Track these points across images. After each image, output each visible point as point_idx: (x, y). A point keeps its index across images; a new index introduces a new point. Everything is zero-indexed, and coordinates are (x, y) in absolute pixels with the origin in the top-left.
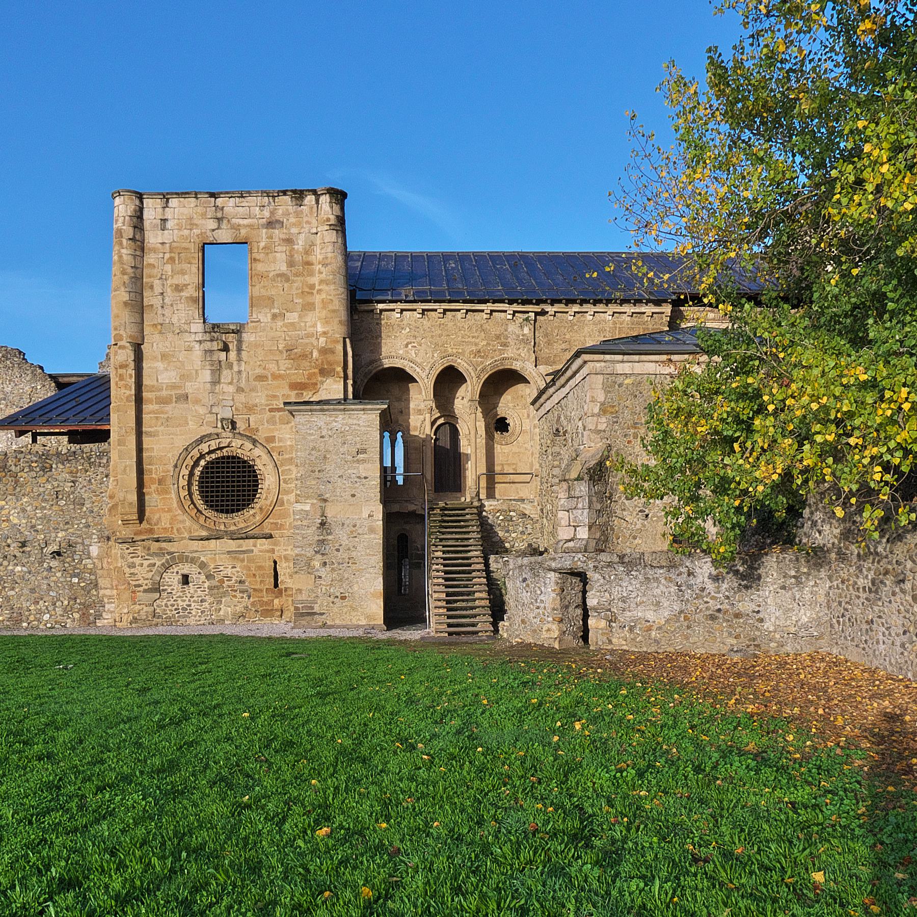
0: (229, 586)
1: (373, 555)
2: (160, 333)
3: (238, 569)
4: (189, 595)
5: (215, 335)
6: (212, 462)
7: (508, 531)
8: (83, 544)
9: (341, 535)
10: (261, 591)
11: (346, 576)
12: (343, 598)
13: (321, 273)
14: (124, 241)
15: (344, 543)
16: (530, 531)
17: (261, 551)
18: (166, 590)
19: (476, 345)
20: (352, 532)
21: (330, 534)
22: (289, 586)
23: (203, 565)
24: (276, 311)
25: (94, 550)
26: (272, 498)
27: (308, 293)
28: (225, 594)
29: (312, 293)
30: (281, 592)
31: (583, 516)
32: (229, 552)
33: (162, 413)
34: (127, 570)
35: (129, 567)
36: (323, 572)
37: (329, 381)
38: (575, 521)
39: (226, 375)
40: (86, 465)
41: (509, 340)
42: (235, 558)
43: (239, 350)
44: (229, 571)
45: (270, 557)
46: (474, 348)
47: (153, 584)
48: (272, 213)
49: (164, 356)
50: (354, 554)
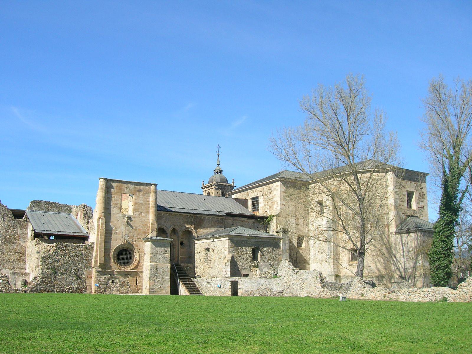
9: (160, 272)
19: (181, 223)
26: (137, 260)
30: (138, 285)
46: (180, 224)
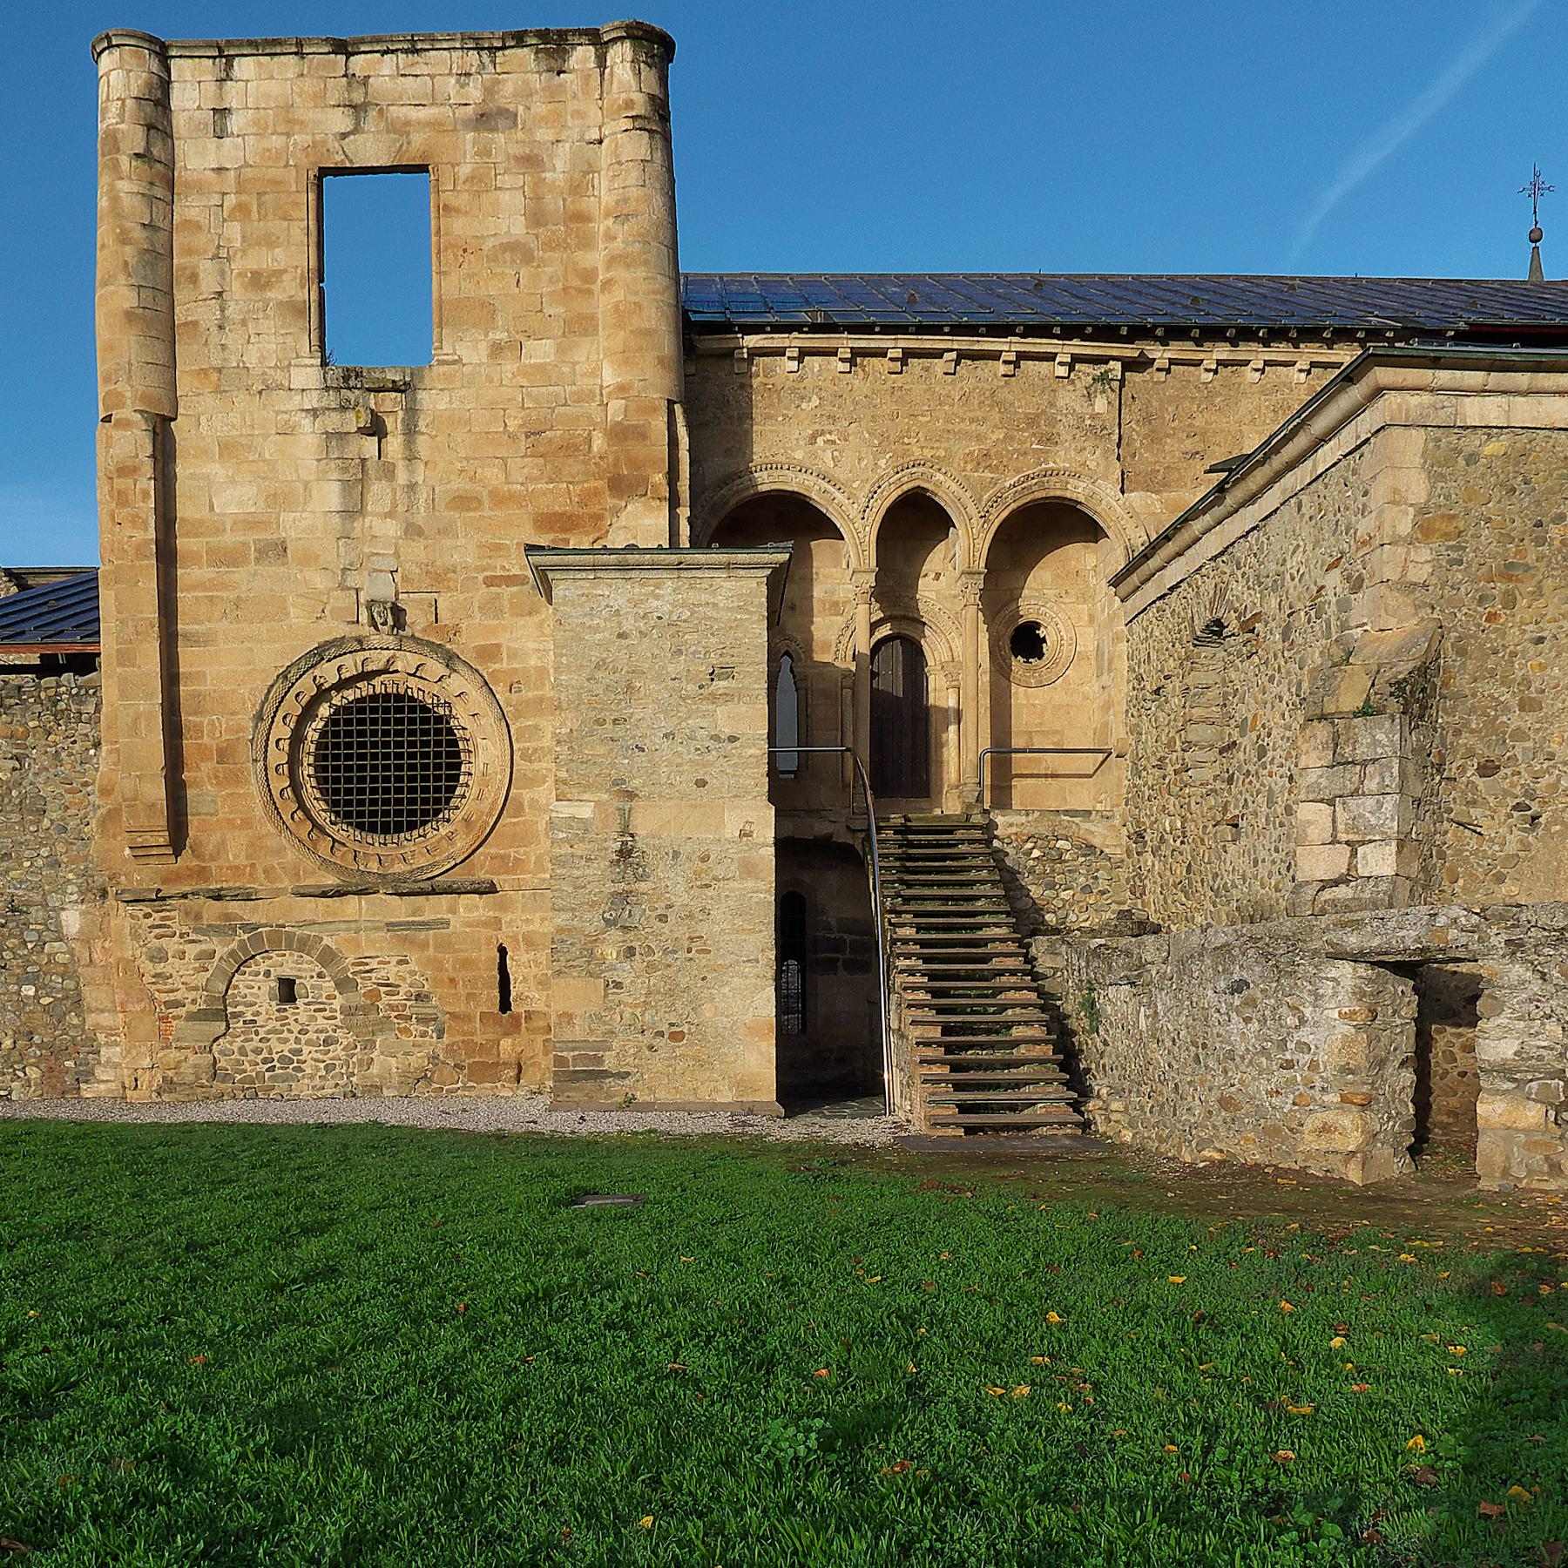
0: (392, 1007)
1: (753, 931)
2: (218, 390)
3: (412, 966)
4: (296, 1028)
5: (352, 396)
6: (347, 709)
8: (44, 905)
9: (670, 882)
10: (467, 1018)
11: (683, 984)
12: (677, 1037)
13: (610, 237)
14: (124, 161)
15: (678, 902)
17: (469, 925)
18: (241, 1014)
21: (639, 879)
22: (535, 1007)
23: (328, 957)
24: (500, 335)
25: (72, 920)
27: (580, 291)
28: (383, 1025)
29: (590, 292)
30: (516, 1020)
31: (1385, 814)
32: (390, 926)
33: (224, 586)
34: (148, 967)
35: (152, 959)
36: (625, 972)
37: (634, 507)
38: (1354, 828)
39: (379, 494)
40: (47, 717)
42: (405, 939)
43: (410, 431)
44: (392, 972)
45: (488, 941)
47: (211, 999)
48: (489, 91)
49: (227, 449)
50: (703, 929)
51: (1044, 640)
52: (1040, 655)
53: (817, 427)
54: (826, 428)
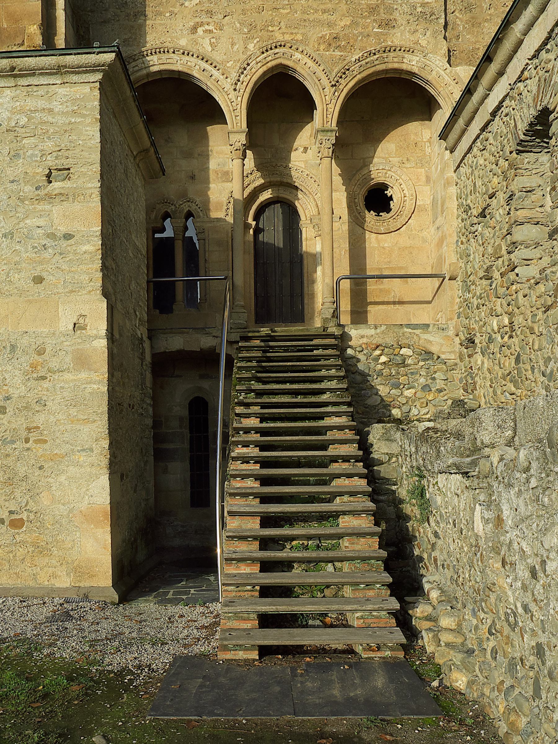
1: (86, 421)
7: (397, 386)
12: (17, 524)
15: (15, 393)
16: (440, 384)
19: (330, 25)
20: (34, 367)
41: (396, 15)
50: (40, 419)
51: (391, 198)
52: (388, 210)
53: (198, 20)
54: (205, 20)
